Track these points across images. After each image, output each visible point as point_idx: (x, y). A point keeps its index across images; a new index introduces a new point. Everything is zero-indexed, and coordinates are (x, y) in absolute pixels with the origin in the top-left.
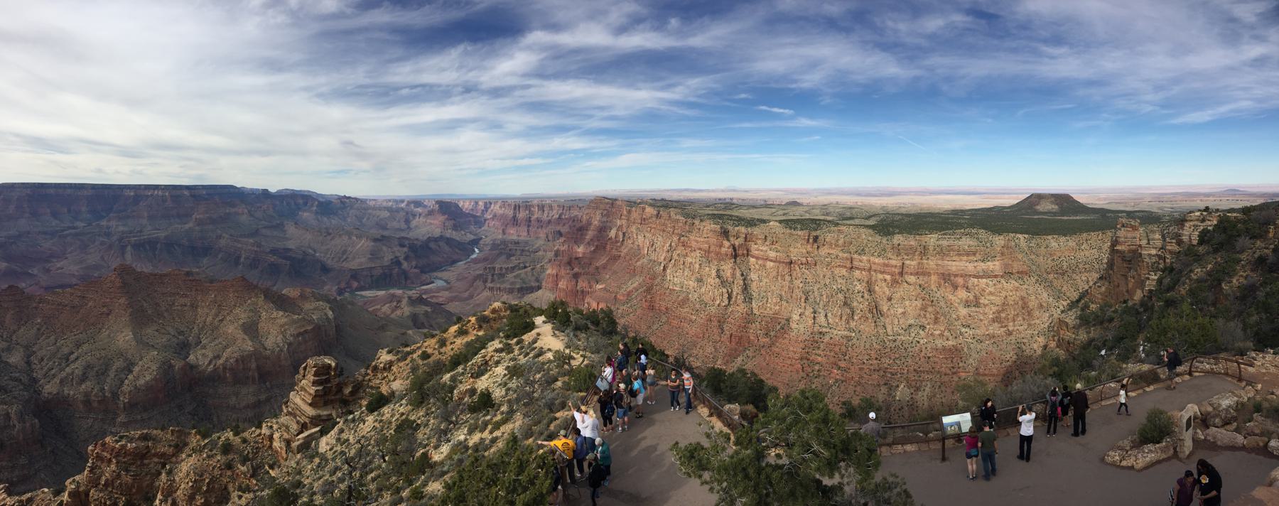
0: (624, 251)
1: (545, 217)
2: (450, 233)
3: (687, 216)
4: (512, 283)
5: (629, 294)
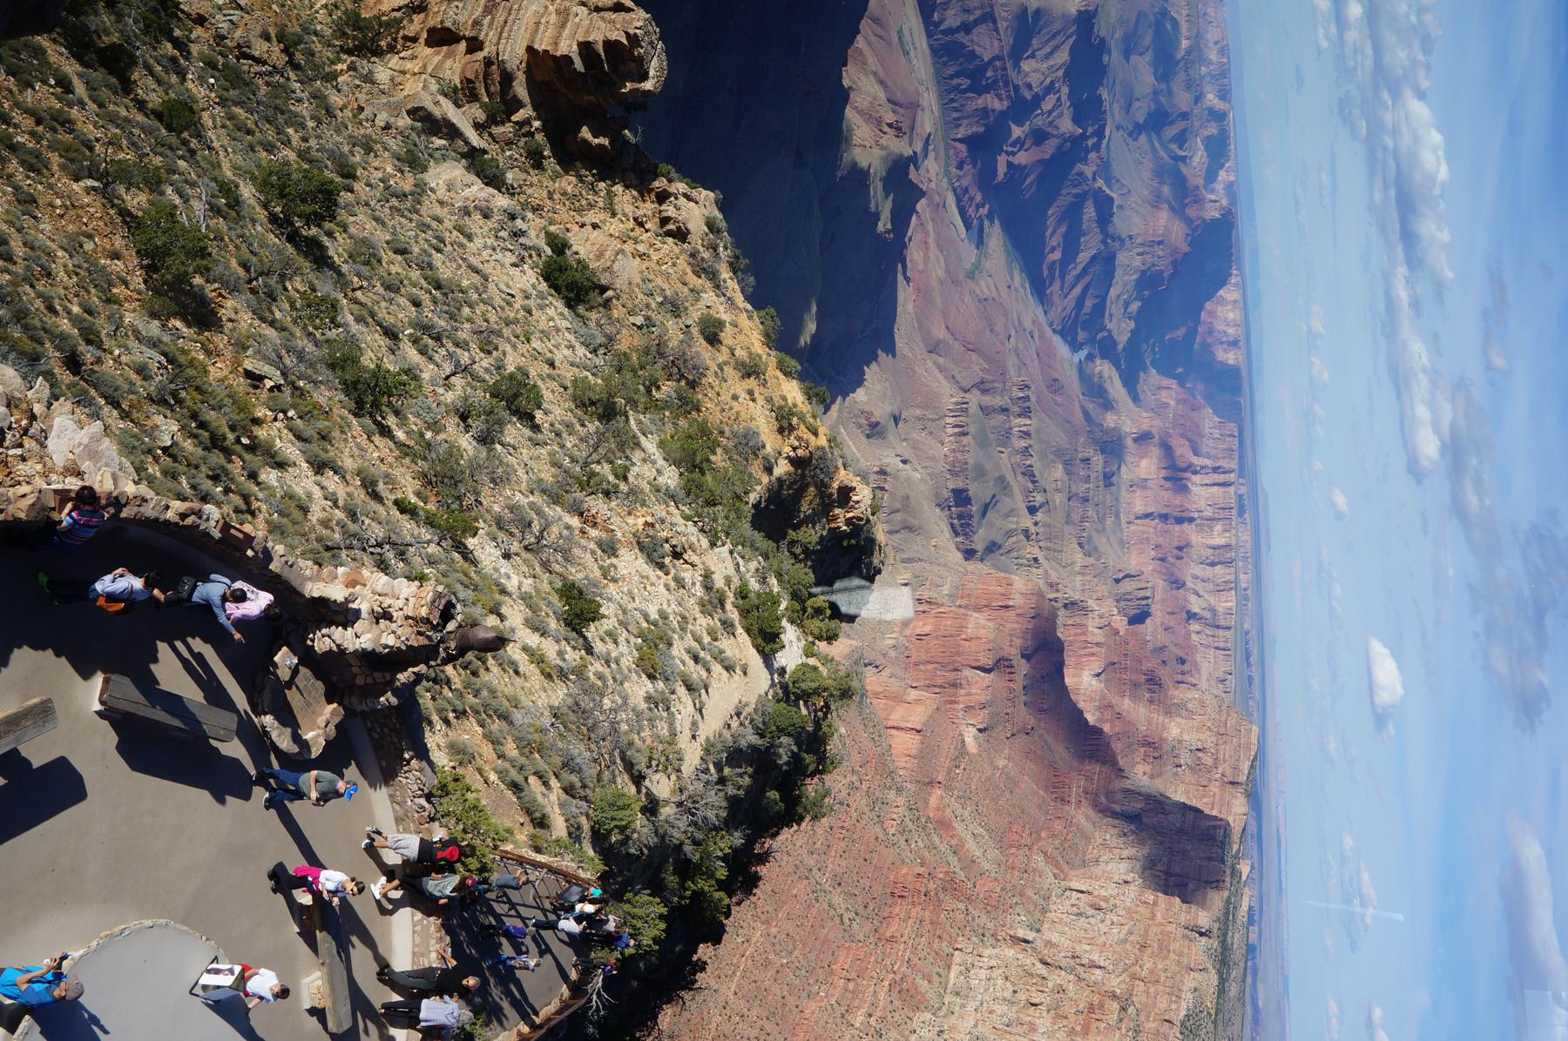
1: (1192, 570)
2: (1129, 263)
5: (944, 825)
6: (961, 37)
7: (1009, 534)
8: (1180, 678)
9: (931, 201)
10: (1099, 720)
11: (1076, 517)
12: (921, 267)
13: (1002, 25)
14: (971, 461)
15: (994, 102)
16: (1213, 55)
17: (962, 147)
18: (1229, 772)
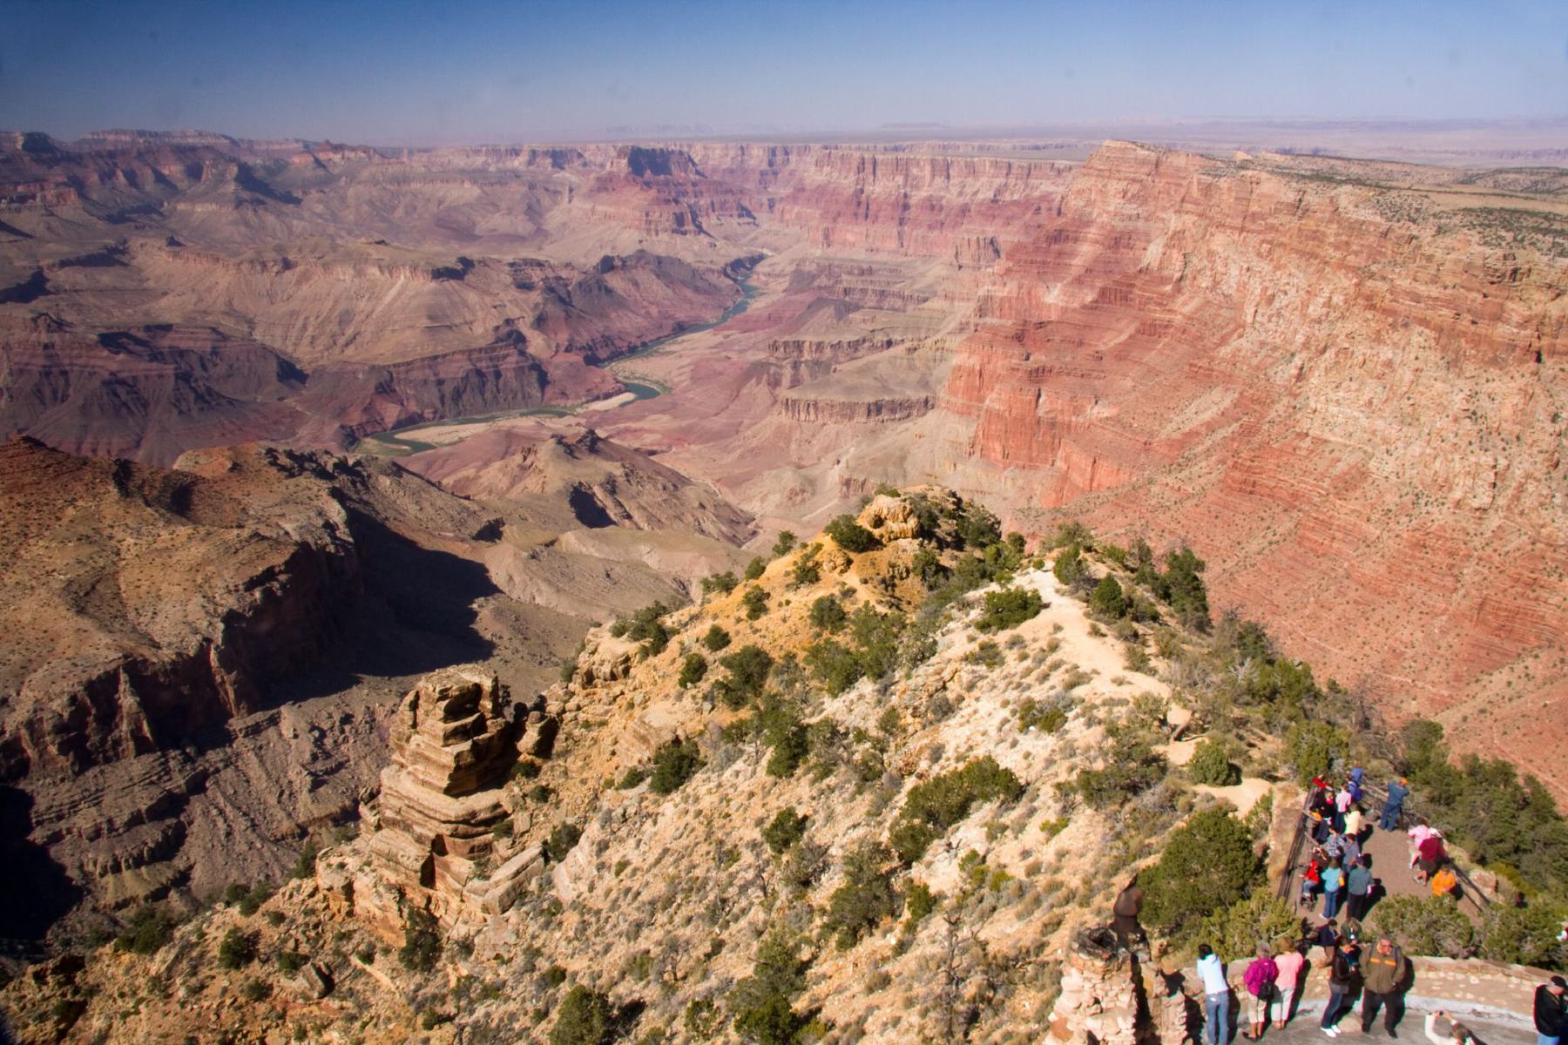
0: (1185, 306)
1: (952, 196)
2: (663, 244)
3: (1394, 212)
4: (850, 390)
6: (448, 389)
7: (911, 368)
8: (1055, 212)
9: (598, 424)
10: (1092, 287)
11: (899, 303)
12: (657, 437)
13: (440, 350)
14: (842, 399)
15: (511, 361)
16: (479, 160)
17: (549, 391)
18: (1145, 169)
